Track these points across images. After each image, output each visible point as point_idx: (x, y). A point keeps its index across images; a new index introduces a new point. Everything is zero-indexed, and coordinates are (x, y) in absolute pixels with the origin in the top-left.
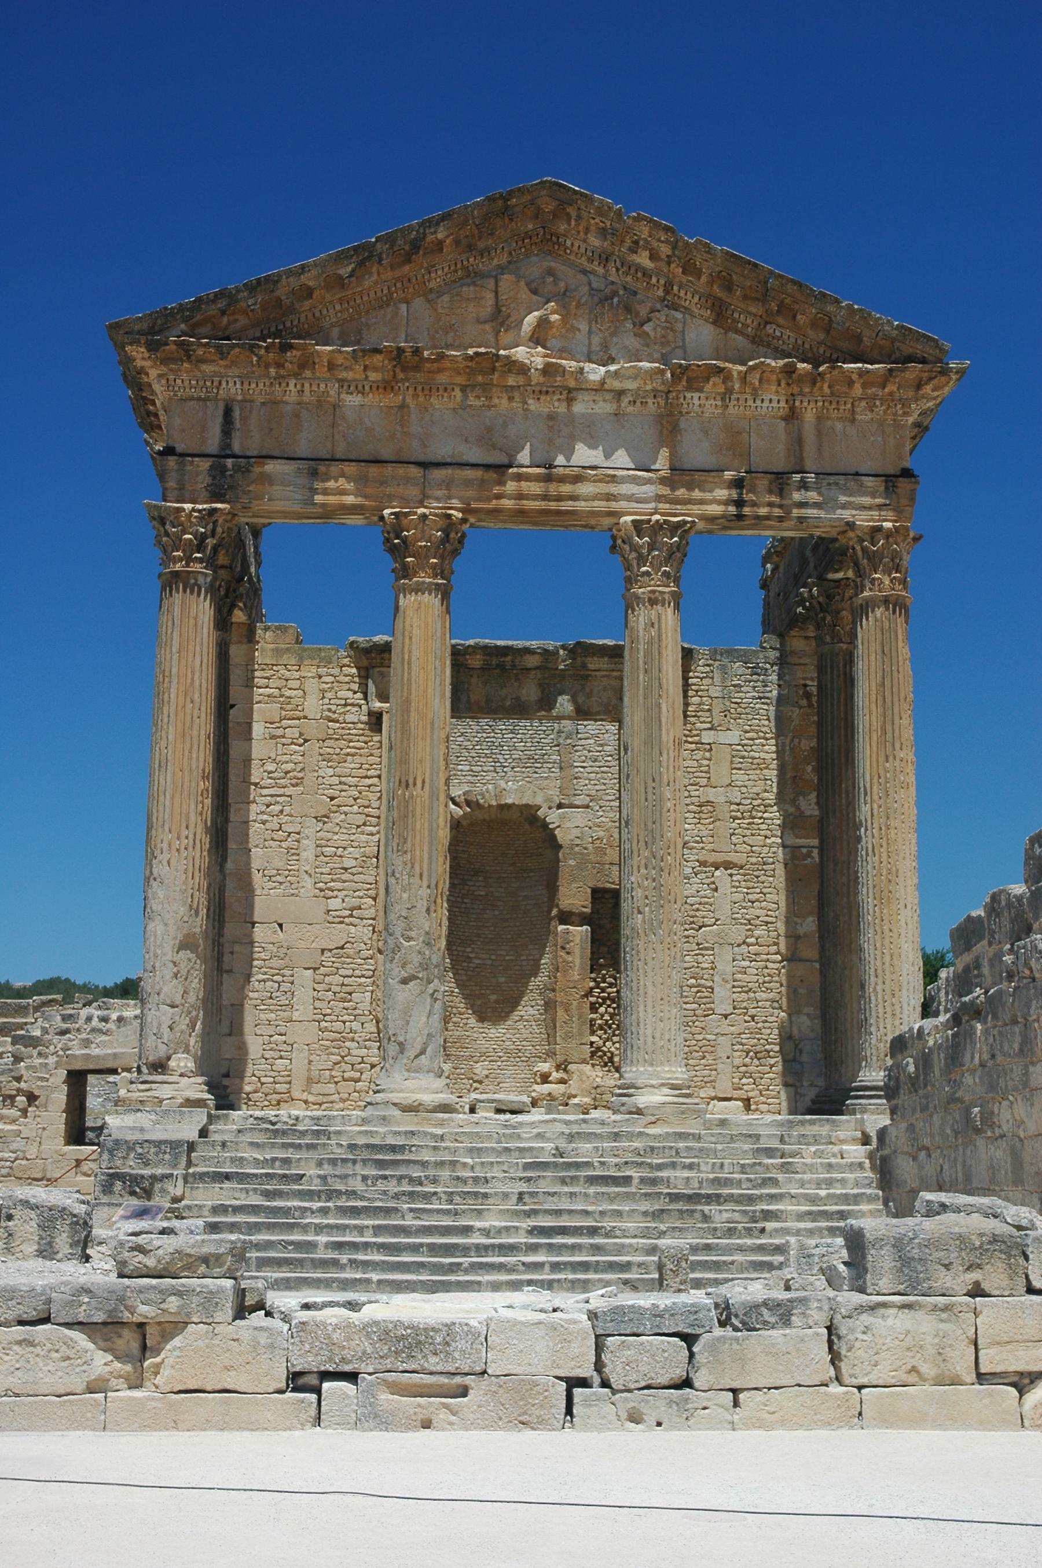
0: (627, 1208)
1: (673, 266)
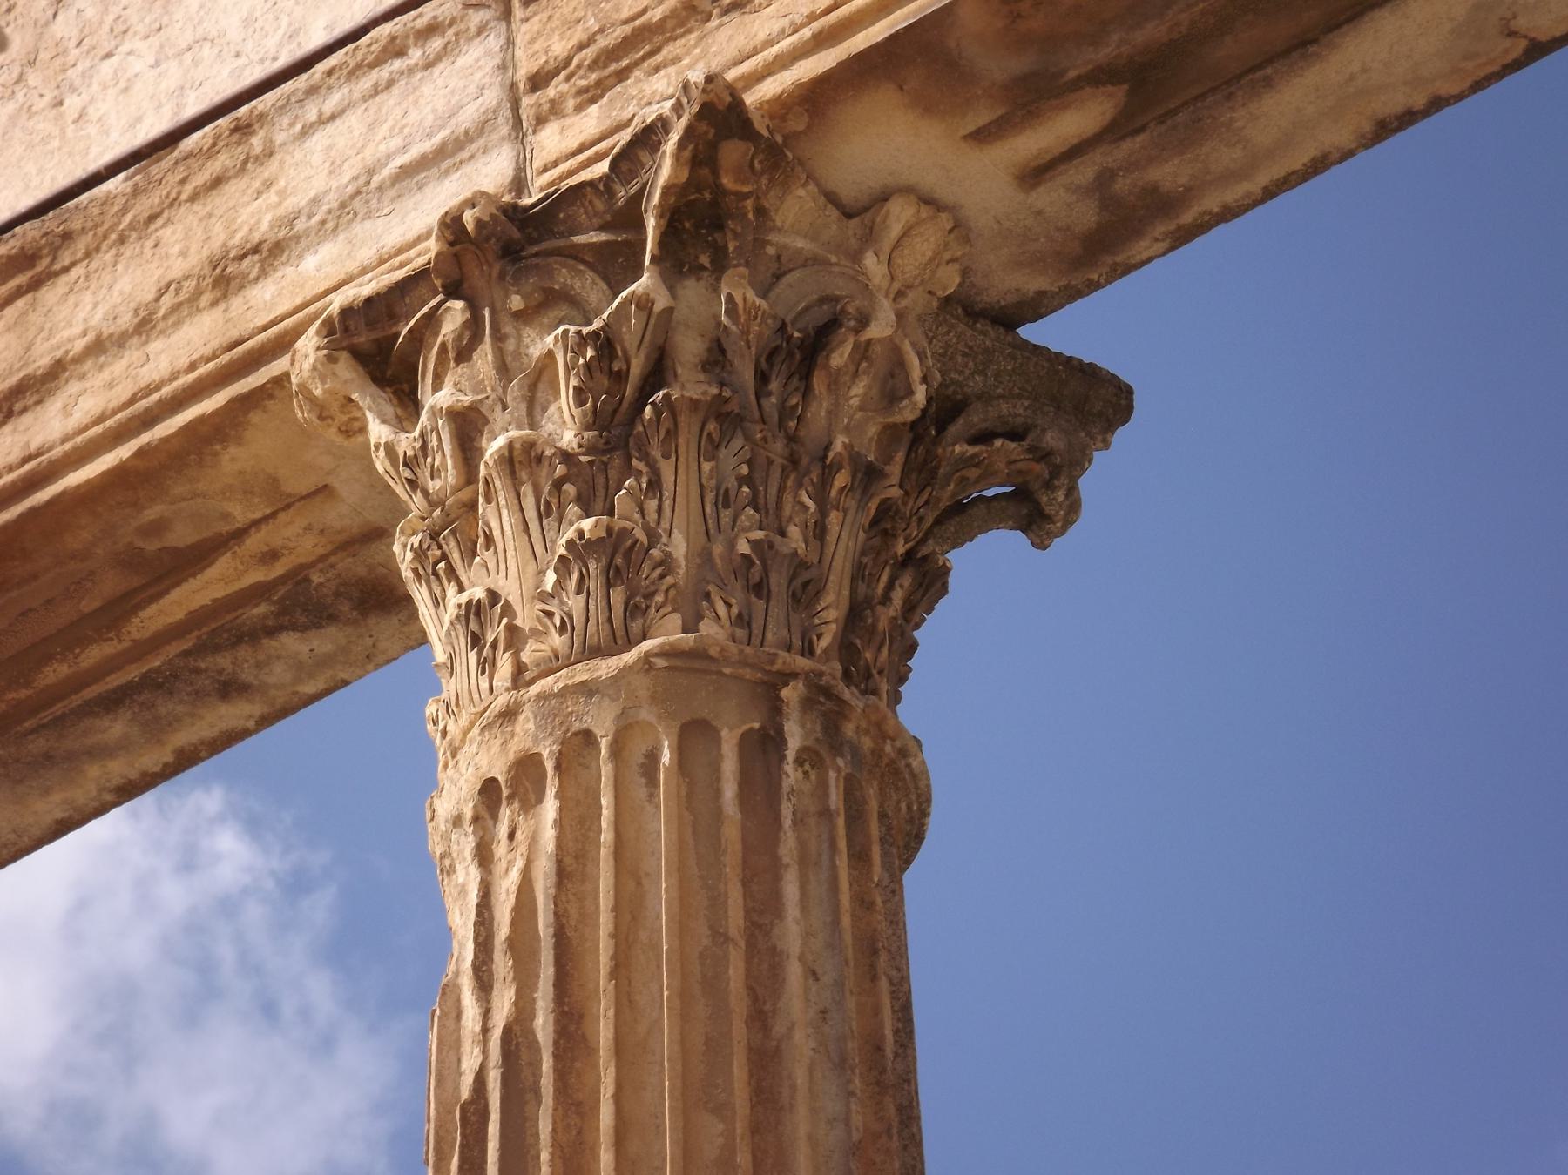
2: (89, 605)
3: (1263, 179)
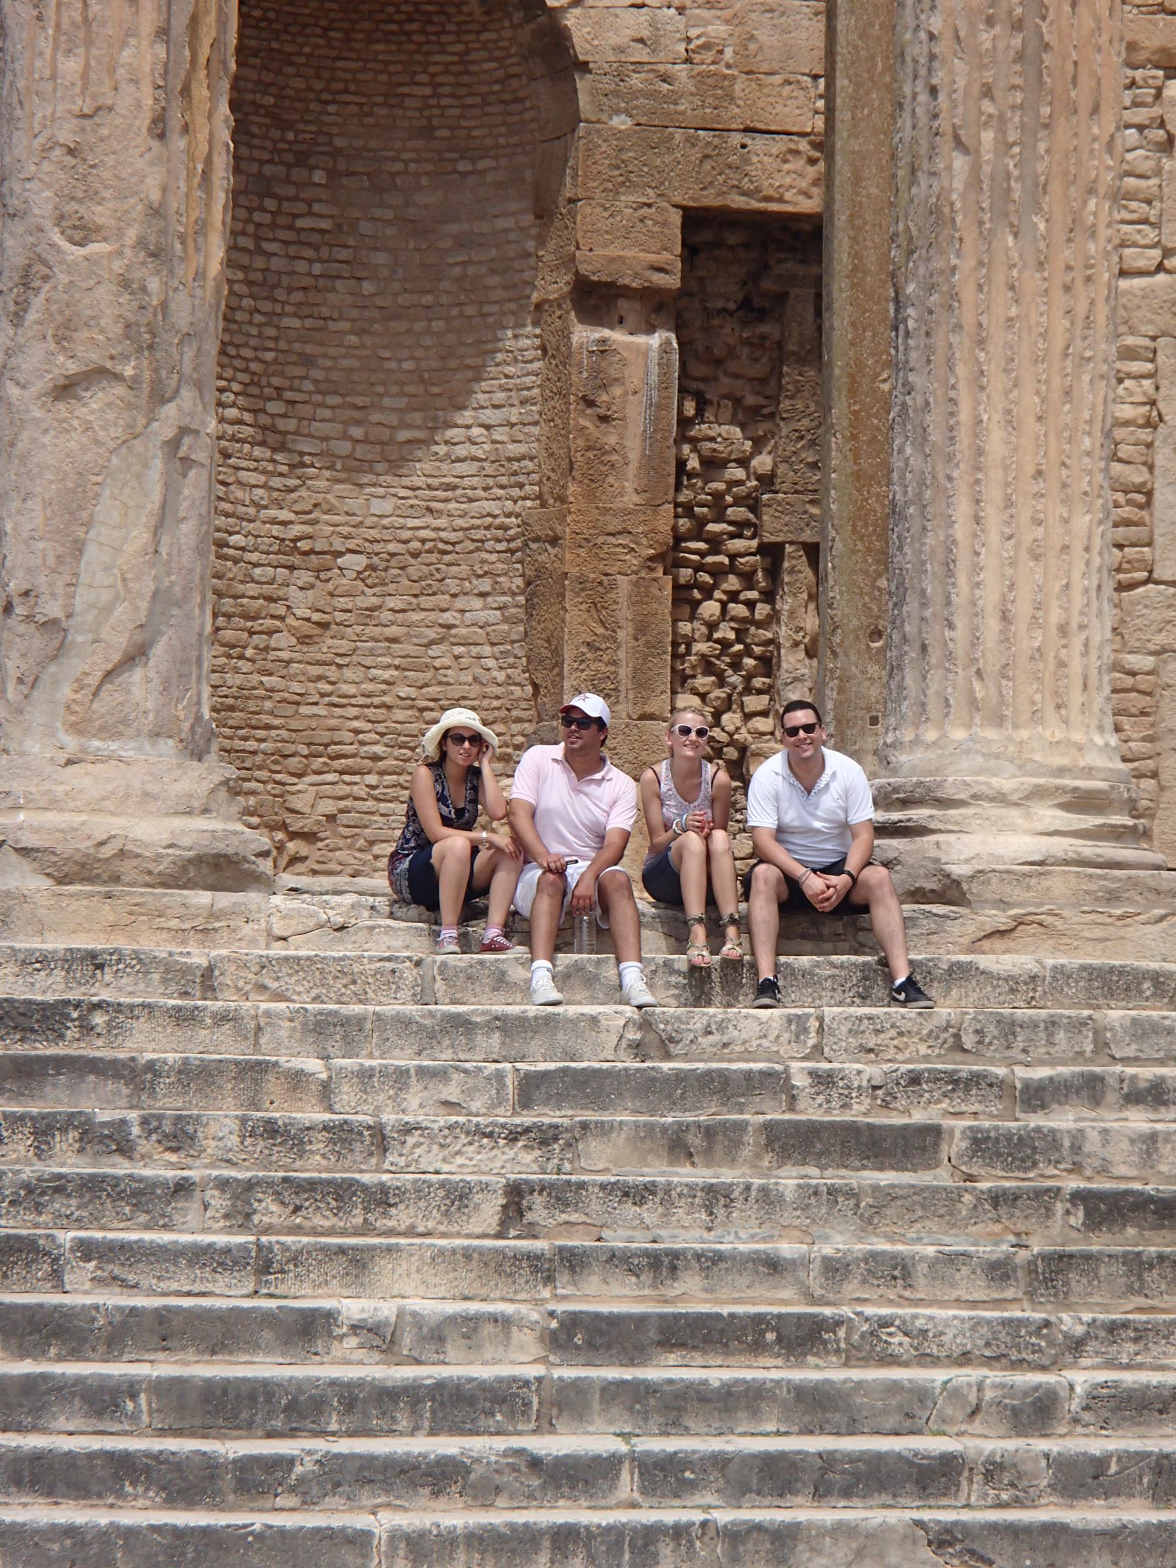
0: (930, 1250)
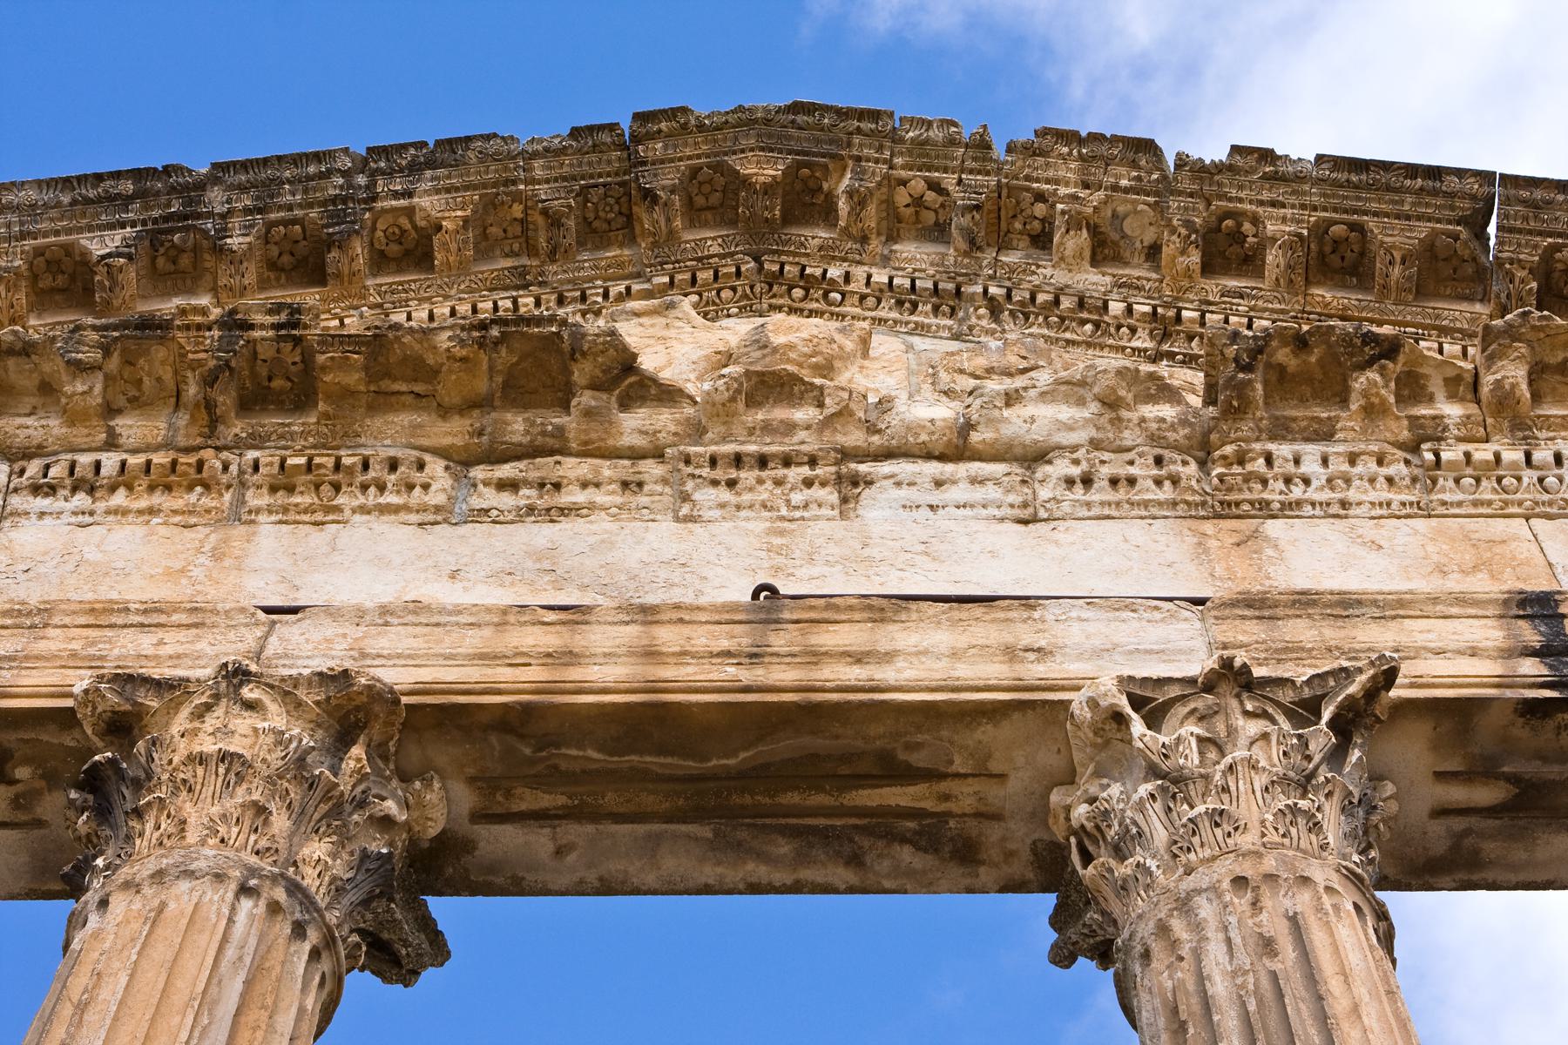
1: (1166, 251)
2: (845, 770)
3: (1522, 877)
